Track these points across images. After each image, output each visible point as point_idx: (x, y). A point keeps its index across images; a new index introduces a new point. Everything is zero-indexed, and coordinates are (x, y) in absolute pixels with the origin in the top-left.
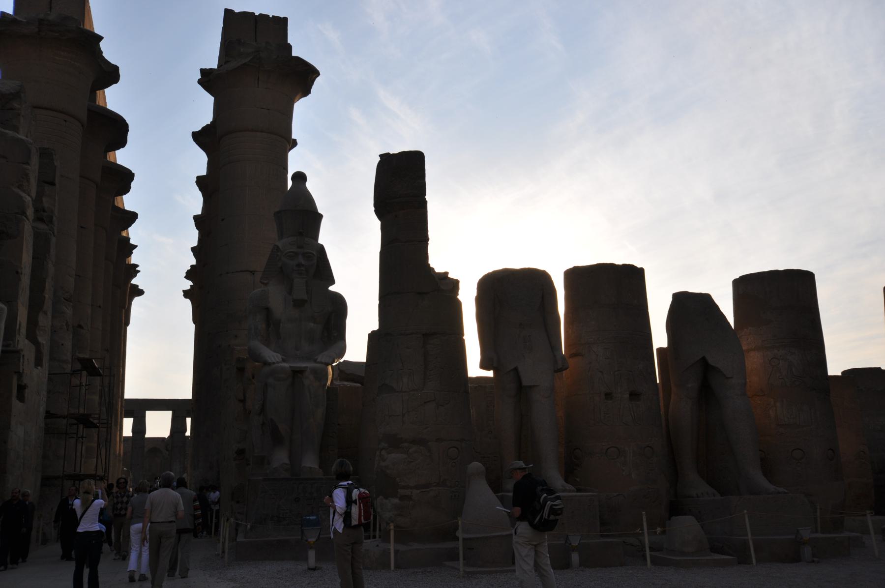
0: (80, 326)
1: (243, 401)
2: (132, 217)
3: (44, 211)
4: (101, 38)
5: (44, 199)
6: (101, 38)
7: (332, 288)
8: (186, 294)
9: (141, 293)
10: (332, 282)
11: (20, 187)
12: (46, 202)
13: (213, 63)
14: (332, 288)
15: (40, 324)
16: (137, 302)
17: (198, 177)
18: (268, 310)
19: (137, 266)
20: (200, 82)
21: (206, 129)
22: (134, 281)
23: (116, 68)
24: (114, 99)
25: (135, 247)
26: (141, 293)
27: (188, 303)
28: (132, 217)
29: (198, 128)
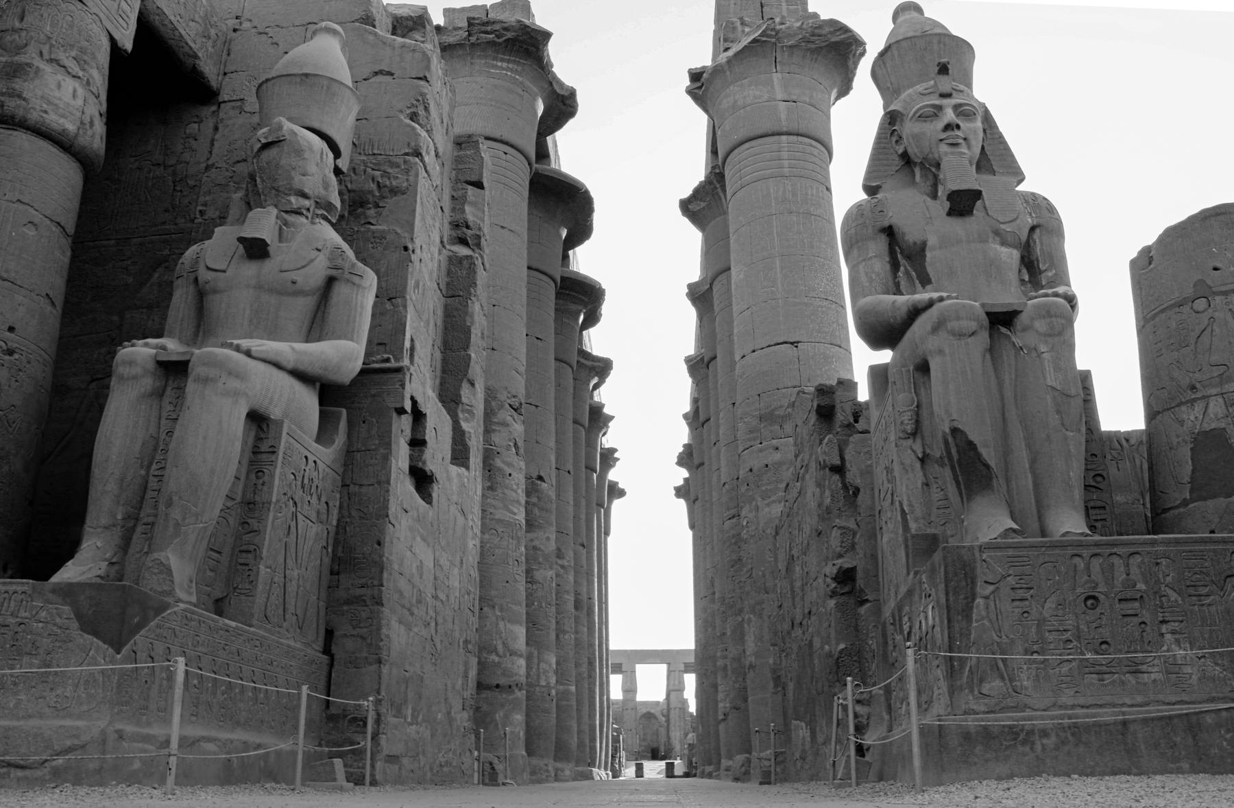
0: (540, 478)
1: (839, 470)
2: (602, 368)
3: (468, 227)
4: (547, 35)
5: (467, 208)
6: (547, 35)
7: (1020, 188)
8: (680, 492)
9: (622, 493)
10: (1021, 178)
11: (414, 117)
12: (470, 214)
13: (704, 58)
14: (1020, 188)
15: (464, 400)
16: (617, 505)
17: (690, 286)
18: (889, 231)
19: (613, 451)
20: (690, 92)
21: (698, 193)
22: (612, 475)
23: (572, 94)
24: (572, 152)
25: (612, 418)
26: (622, 493)
27: (682, 504)
28: (602, 368)
29: (687, 193)
